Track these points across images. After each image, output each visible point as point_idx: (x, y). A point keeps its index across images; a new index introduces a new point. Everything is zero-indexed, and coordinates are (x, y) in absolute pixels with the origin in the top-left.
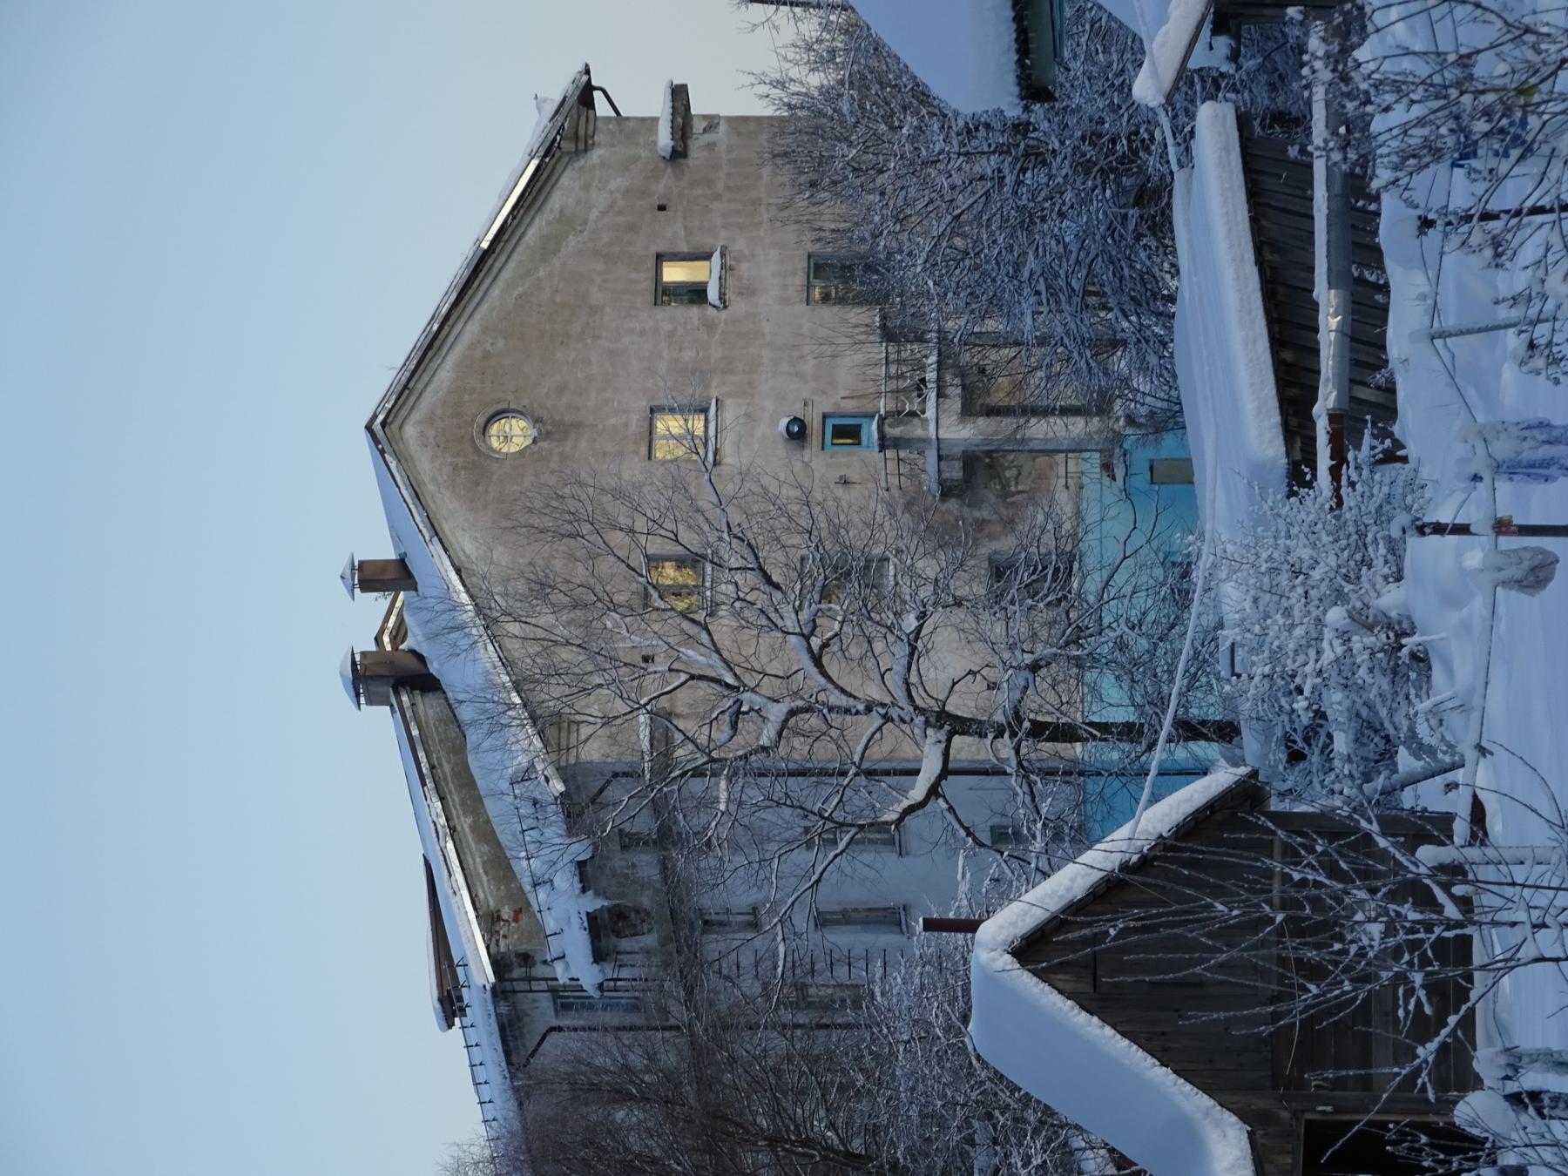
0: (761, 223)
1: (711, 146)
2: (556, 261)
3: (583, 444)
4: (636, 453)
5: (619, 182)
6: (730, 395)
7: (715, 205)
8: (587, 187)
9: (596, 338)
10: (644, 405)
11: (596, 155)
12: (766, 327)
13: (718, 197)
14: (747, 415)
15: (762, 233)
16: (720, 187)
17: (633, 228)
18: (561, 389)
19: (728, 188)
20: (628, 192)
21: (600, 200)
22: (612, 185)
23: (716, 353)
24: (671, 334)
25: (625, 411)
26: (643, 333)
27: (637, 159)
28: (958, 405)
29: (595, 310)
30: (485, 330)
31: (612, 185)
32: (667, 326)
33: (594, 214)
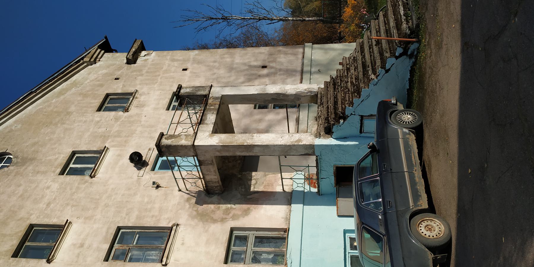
0: (156, 83)
1: (146, 60)
2: (62, 97)
3: (31, 168)
4: (54, 172)
5: (104, 71)
6: (113, 146)
7: (140, 77)
8: (89, 74)
9: (64, 124)
10: (69, 151)
11: (98, 64)
12: (143, 119)
13: (142, 75)
14: (119, 155)
15: (156, 86)
16: (144, 72)
17: (101, 85)
18: (34, 144)
19: (147, 72)
20: (107, 73)
21: (92, 77)
22: (100, 72)
23: (116, 128)
24: (98, 122)
25: (59, 153)
26: (85, 122)
27: (113, 65)
28: (211, 127)
29: (69, 114)
30: (16, 122)
31: (100, 72)
32: (98, 119)
33: (88, 81)
